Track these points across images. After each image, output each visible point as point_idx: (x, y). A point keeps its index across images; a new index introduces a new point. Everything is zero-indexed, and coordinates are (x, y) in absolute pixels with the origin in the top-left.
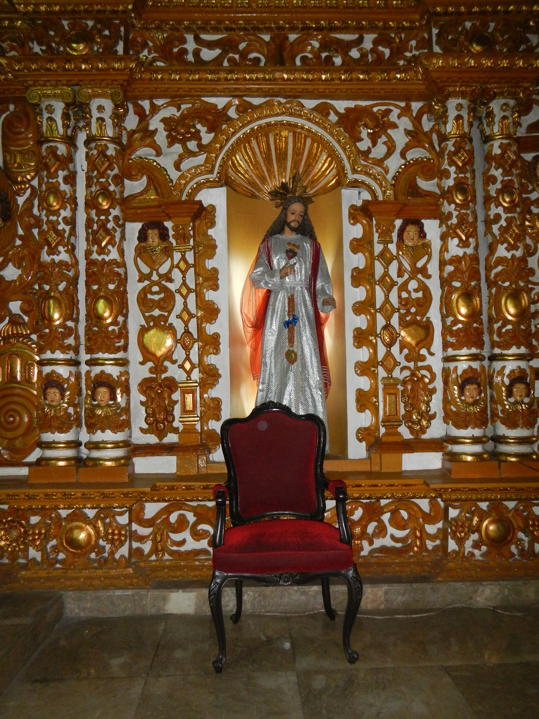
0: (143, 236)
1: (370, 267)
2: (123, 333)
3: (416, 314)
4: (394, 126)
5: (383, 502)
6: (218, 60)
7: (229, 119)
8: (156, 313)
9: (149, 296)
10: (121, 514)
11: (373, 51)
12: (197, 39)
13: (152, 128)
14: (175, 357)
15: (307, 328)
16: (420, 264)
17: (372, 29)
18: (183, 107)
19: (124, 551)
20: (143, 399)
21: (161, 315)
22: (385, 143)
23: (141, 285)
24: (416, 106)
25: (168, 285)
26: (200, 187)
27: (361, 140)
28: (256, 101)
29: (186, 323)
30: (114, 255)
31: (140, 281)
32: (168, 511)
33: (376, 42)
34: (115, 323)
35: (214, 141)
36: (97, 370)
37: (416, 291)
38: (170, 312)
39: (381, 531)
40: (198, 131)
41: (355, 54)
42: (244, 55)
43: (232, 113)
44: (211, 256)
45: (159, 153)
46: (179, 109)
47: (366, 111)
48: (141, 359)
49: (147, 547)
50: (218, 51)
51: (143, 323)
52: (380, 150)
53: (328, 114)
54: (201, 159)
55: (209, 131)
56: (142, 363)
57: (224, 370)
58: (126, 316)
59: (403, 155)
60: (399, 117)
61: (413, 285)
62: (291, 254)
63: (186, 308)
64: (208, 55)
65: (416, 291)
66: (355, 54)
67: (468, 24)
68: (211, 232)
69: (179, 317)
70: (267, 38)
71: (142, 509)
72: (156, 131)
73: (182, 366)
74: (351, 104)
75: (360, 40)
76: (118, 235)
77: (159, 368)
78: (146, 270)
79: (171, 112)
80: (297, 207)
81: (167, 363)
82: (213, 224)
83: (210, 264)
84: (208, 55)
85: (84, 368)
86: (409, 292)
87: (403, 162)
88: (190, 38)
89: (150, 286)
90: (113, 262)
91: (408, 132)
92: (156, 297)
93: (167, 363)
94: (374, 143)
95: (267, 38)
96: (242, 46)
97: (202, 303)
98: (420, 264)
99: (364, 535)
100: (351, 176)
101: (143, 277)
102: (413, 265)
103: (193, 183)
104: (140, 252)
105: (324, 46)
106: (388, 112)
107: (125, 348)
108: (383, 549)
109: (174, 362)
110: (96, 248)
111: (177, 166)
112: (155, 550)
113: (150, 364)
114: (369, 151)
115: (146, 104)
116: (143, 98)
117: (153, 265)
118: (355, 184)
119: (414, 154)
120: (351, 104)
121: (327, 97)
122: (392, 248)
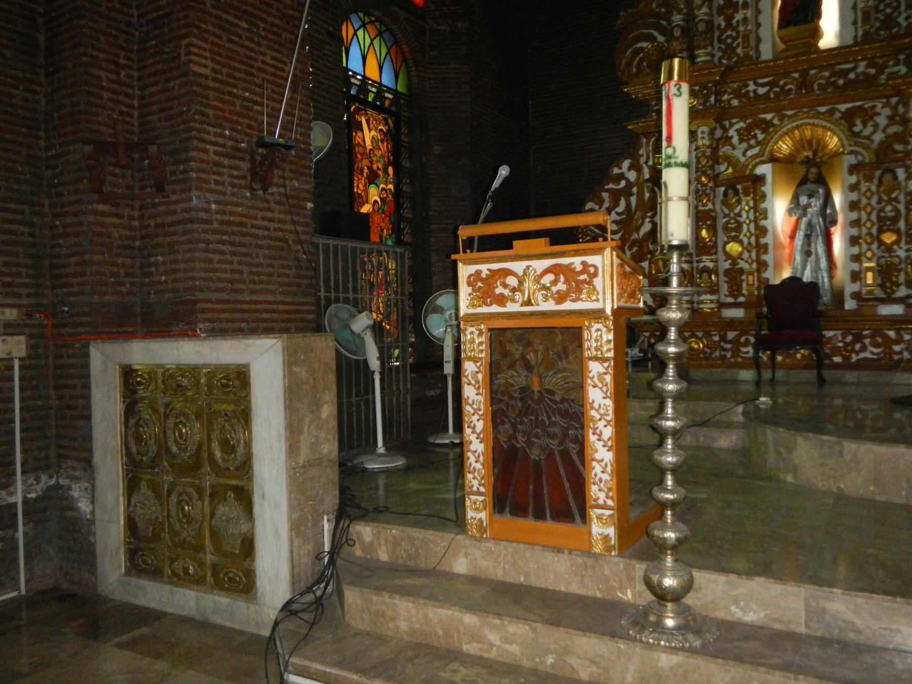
1: (859, 201)
2: (715, 245)
3: (890, 225)
5: (866, 332)
6: (767, 93)
7: (774, 125)
8: (733, 234)
9: (730, 226)
10: (715, 335)
12: (756, 84)
13: (730, 135)
14: (743, 257)
15: (820, 239)
16: (893, 195)
18: (748, 121)
19: (717, 354)
20: (726, 279)
21: (735, 236)
22: (872, 126)
23: (725, 220)
24: (894, 100)
25: (739, 219)
27: (855, 125)
28: (790, 113)
29: (749, 238)
30: (710, 206)
31: (724, 217)
32: (740, 336)
33: (867, 67)
34: (711, 241)
35: (764, 139)
36: (702, 265)
37: (891, 211)
38: (740, 233)
39: (864, 349)
40: (756, 134)
41: (852, 76)
42: (782, 88)
43: (776, 121)
44: (764, 201)
46: (745, 122)
47: (860, 108)
48: (724, 258)
49: (729, 355)
51: (726, 239)
52: (869, 130)
53: (834, 114)
54: (756, 150)
55: (762, 133)
56: (725, 261)
58: (716, 237)
59: (884, 131)
60: (882, 108)
62: (810, 196)
63: (749, 230)
64: (762, 91)
66: (852, 76)
68: (763, 188)
69: (745, 235)
70: (796, 75)
71: (726, 335)
72: (732, 137)
73: (747, 261)
74: (849, 105)
75: (855, 67)
76: (712, 196)
77: (734, 263)
78: (727, 211)
79: (742, 124)
80: (814, 170)
81: (739, 261)
83: (763, 205)
85: (695, 264)
87: (884, 135)
88: (751, 83)
90: (710, 210)
92: (733, 226)
93: (739, 261)
96: (782, 83)
97: (757, 227)
98: (893, 195)
99: (853, 351)
104: (725, 203)
105: (833, 74)
106: (874, 107)
107: (716, 253)
108: (865, 359)
109: (742, 259)
110: (700, 204)
111: (744, 154)
112: (733, 356)
113: (730, 261)
115: (727, 124)
117: (731, 207)
118: (851, 153)
119: (892, 130)
120: (849, 105)
122: (874, 188)
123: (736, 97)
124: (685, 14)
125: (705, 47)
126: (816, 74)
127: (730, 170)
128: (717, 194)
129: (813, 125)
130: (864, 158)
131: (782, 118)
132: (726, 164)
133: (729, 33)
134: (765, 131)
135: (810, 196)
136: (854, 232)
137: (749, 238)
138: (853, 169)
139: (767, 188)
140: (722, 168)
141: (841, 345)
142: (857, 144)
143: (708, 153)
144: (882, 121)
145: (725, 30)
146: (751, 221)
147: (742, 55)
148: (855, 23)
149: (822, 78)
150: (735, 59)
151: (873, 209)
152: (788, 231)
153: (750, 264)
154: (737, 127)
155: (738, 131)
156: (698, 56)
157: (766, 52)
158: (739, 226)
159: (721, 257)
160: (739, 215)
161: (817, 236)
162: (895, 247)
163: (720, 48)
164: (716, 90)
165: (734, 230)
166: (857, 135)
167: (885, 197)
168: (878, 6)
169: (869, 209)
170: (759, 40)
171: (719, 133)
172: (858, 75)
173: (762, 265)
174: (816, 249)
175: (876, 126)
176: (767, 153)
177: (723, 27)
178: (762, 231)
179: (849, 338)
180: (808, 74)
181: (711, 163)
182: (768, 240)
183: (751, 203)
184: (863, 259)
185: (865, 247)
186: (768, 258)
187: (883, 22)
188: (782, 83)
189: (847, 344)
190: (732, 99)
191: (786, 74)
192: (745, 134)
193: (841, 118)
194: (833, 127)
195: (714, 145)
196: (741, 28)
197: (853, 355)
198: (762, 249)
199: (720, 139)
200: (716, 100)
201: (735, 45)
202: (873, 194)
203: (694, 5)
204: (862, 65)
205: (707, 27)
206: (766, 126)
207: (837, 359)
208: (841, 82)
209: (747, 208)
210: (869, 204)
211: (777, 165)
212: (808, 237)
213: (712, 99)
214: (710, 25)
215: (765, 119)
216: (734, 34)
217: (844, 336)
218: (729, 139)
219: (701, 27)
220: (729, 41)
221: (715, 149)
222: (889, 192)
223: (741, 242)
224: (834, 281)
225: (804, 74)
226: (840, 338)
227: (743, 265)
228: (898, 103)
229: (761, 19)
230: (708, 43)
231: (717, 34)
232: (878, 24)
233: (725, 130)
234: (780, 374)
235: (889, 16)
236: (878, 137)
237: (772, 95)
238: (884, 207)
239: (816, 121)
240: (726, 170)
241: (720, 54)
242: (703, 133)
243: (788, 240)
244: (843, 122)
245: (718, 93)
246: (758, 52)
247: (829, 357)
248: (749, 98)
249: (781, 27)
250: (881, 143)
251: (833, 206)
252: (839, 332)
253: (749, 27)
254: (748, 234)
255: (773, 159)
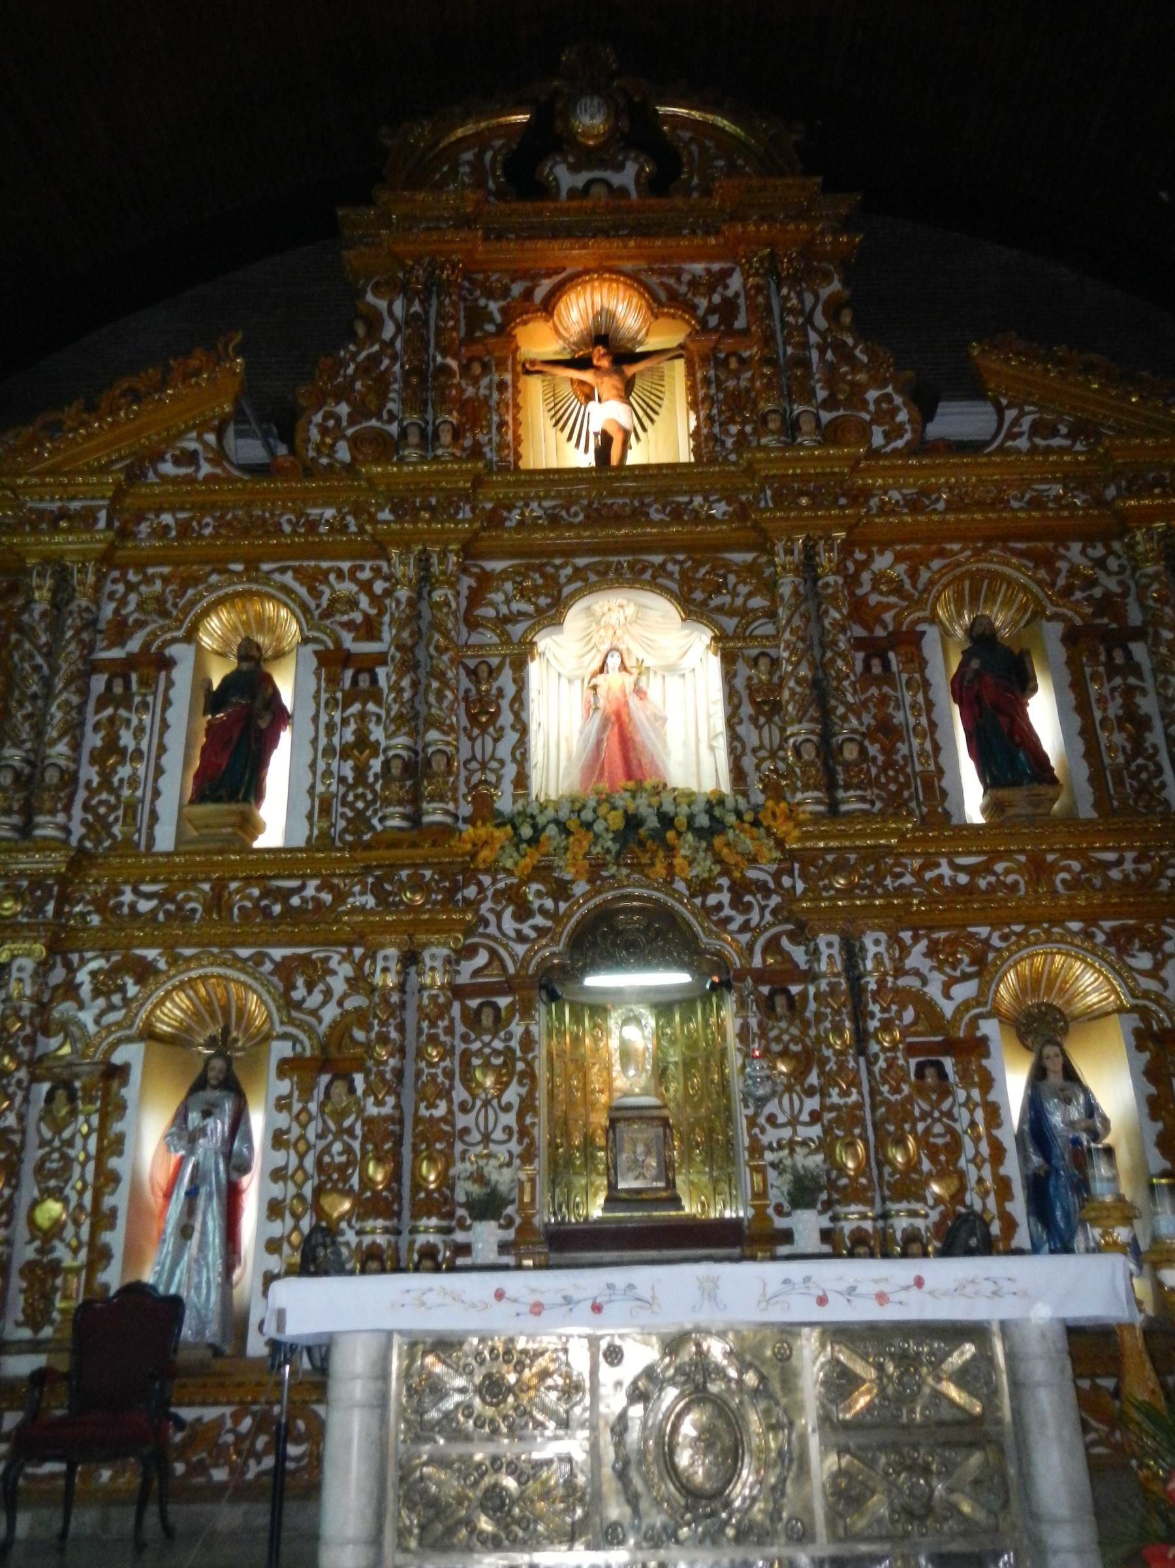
0: (50, 1098)
3: (338, 1181)
4: (333, 973)
6: (154, 912)
8: (53, 1183)
11: (314, 898)
12: (136, 891)
16: (347, 1123)
17: (313, 876)
20: (24, 1285)
23: (41, 1152)
24: (358, 951)
26: (114, 1046)
27: (294, 988)
28: (188, 952)
31: (41, 1146)
33: (319, 889)
37: (340, 1154)
38: (67, 1181)
40: (125, 984)
41: (295, 901)
43: (162, 965)
44: (121, 1117)
45: (81, 1006)
46: (108, 960)
47: (307, 958)
48: (27, 1236)
50: (154, 903)
52: (316, 998)
53: (261, 963)
57: (118, 1250)
58: (16, 1188)
59: (340, 1004)
60: (340, 963)
61: (337, 1147)
63: (82, 1177)
64: (144, 906)
65: (340, 1154)
66: (295, 901)
67: (404, 874)
70: (206, 887)
72: (81, 984)
73: (68, 1245)
74: (288, 951)
78: (47, 1134)
82: (124, 1082)
83: (118, 1127)
84: (144, 906)
86: (332, 1157)
87: (339, 1011)
88: (128, 889)
89: (50, 1153)
90: (8, 1130)
91: (348, 980)
92: (55, 1165)
93: (56, 1243)
94: (310, 992)
95: (206, 887)
97: (97, 1174)
98: (347, 1123)
100: (279, 1029)
101: (43, 1143)
102: (339, 1124)
103: (111, 1039)
104: (47, 1114)
105: (266, 893)
106: (328, 959)
109: (62, 1240)
111: (97, 1022)
113: (37, 1243)
114: (304, 1000)
115: (75, 958)
116: (73, 951)
118: (284, 1037)
119: (349, 1004)
120: (288, 951)
121: (261, 945)
122: (313, 1107)
123: (99, 911)
124: (27, 751)
125: (53, 812)
126: (237, 891)
127: (66, 1050)
128: (32, 1097)
129: (227, 979)
130: (304, 1049)
131: (174, 960)
132: (61, 1036)
133: (104, 796)
134: (140, 980)
135: (206, 1114)
136: (277, 1190)
137: (81, 1193)
138: (286, 1067)
139: (130, 1093)
140: (54, 1042)
141: (230, 1438)
142: (292, 1022)
143: (26, 1012)
144: (338, 985)
145: (93, 792)
146: (88, 1158)
147: (120, 837)
148: (310, 817)
149: (249, 897)
150: (107, 844)
151: (309, 1147)
152: (162, 1179)
153: (75, 1251)
154: (94, 965)
155: (94, 974)
156: (38, 826)
157: (165, 838)
158: (67, 1161)
159: (21, 1231)
160: (70, 1143)
161: (210, 1197)
162: (343, 1225)
163: (84, 822)
164: (62, 892)
165: (54, 1174)
166: (298, 1005)
167: (332, 1126)
168: (345, 796)
169: (302, 1146)
170: (154, 817)
171: (58, 975)
172: (304, 901)
173: (100, 1255)
174: (204, 1223)
175: (328, 993)
176: (139, 1023)
177: (95, 784)
178: (107, 1179)
179: (247, 1423)
180: (226, 887)
181: (28, 1030)
182: (118, 1199)
183: (95, 1120)
184: (286, 1249)
185: (289, 1221)
186: (115, 1239)
187: (349, 821)
188: (180, 896)
189: (240, 1438)
190: (89, 913)
191: (186, 884)
192: (104, 986)
193: (272, 973)
194: (256, 985)
195: (46, 999)
196: (126, 792)
197: (252, 1462)
198: (103, 1219)
199: (56, 988)
200: (58, 912)
201: (111, 819)
202: (311, 1118)
203: (46, 738)
204: (313, 884)
205: (62, 778)
206: (144, 972)
207: (220, 1475)
208: (277, 909)
209: (85, 1129)
210: (302, 1137)
211: (156, 1046)
212: (192, 1194)
213: (50, 908)
214: (70, 779)
215: (144, 958)
216: (112, 799)
217: (237, 1418)
218: (70, 989)
219: (52, 776)
220: (102, 810)
221: (42, 1008)
222: (340, 1115)
223: (65, 1201)
224: (236, 1292)
225: (220, 886)
226: (229, 1424)
227: (61, 1252)
228: (364, 958)
229: (163, 783)
230: (59, 806)
231: (82, 795)
232: (342, 824)
233: (71, 970)
234: (85, 1519)
235: (360, 814)
236: (330, 1013)
237: (161, 917)
238: (330, 1145)
239: (230, 972)
240: (60, 1047)
241: (83, 830)
242: (20, 969)
243: (160, 1200)
244: (275, 979)
245: (64, 899)
246: (151, 839)
247: (201, 1468)
248: (121, 916)
249: (192, 802)
250: (334, 1026)
251: (248, 1138)
252: (228, 1410)
253: (139, 793)
254: (79, 1185)
255: (149, 1035)
